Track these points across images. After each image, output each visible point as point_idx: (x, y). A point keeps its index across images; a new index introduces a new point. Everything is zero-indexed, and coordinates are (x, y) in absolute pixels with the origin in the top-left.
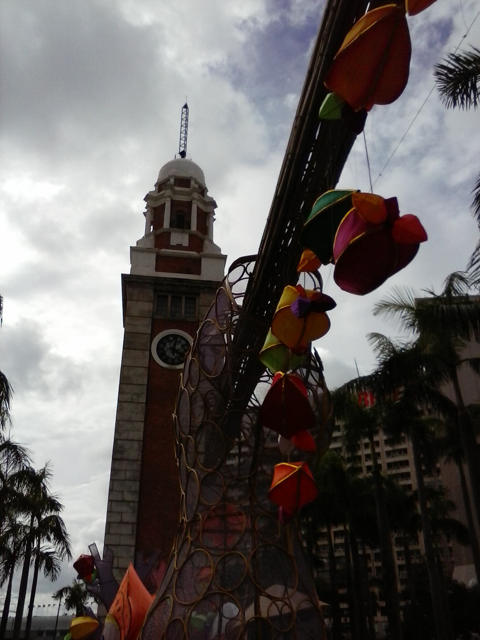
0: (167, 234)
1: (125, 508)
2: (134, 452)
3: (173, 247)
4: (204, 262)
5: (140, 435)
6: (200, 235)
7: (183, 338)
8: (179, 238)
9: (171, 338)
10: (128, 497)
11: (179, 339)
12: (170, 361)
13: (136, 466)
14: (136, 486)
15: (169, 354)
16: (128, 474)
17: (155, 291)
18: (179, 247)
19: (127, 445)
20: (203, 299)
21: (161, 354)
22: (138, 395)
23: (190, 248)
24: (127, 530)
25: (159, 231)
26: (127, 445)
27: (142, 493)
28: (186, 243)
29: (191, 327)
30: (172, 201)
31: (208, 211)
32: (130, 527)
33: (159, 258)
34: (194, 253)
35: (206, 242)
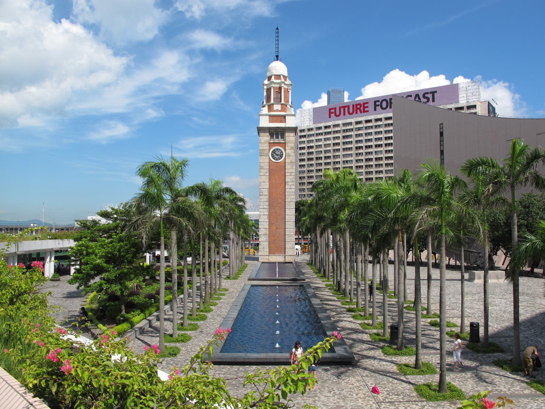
1: (264, 210)
3: (275, 111)
5: (268, 187)
6: (286, 103)
8: (277, 107)
10: (265, 207)
13: (267, 197)
15: (275, 156)
16: (265, 200)
18: (277, 111)
20: (287, 134)
21: (273, 157)
22: (266, 173)
23: (282, 110)
24: (266, 217)
25: (269, 104)
27: (270, 205)
28: (280, 109)
34: (283, 113)
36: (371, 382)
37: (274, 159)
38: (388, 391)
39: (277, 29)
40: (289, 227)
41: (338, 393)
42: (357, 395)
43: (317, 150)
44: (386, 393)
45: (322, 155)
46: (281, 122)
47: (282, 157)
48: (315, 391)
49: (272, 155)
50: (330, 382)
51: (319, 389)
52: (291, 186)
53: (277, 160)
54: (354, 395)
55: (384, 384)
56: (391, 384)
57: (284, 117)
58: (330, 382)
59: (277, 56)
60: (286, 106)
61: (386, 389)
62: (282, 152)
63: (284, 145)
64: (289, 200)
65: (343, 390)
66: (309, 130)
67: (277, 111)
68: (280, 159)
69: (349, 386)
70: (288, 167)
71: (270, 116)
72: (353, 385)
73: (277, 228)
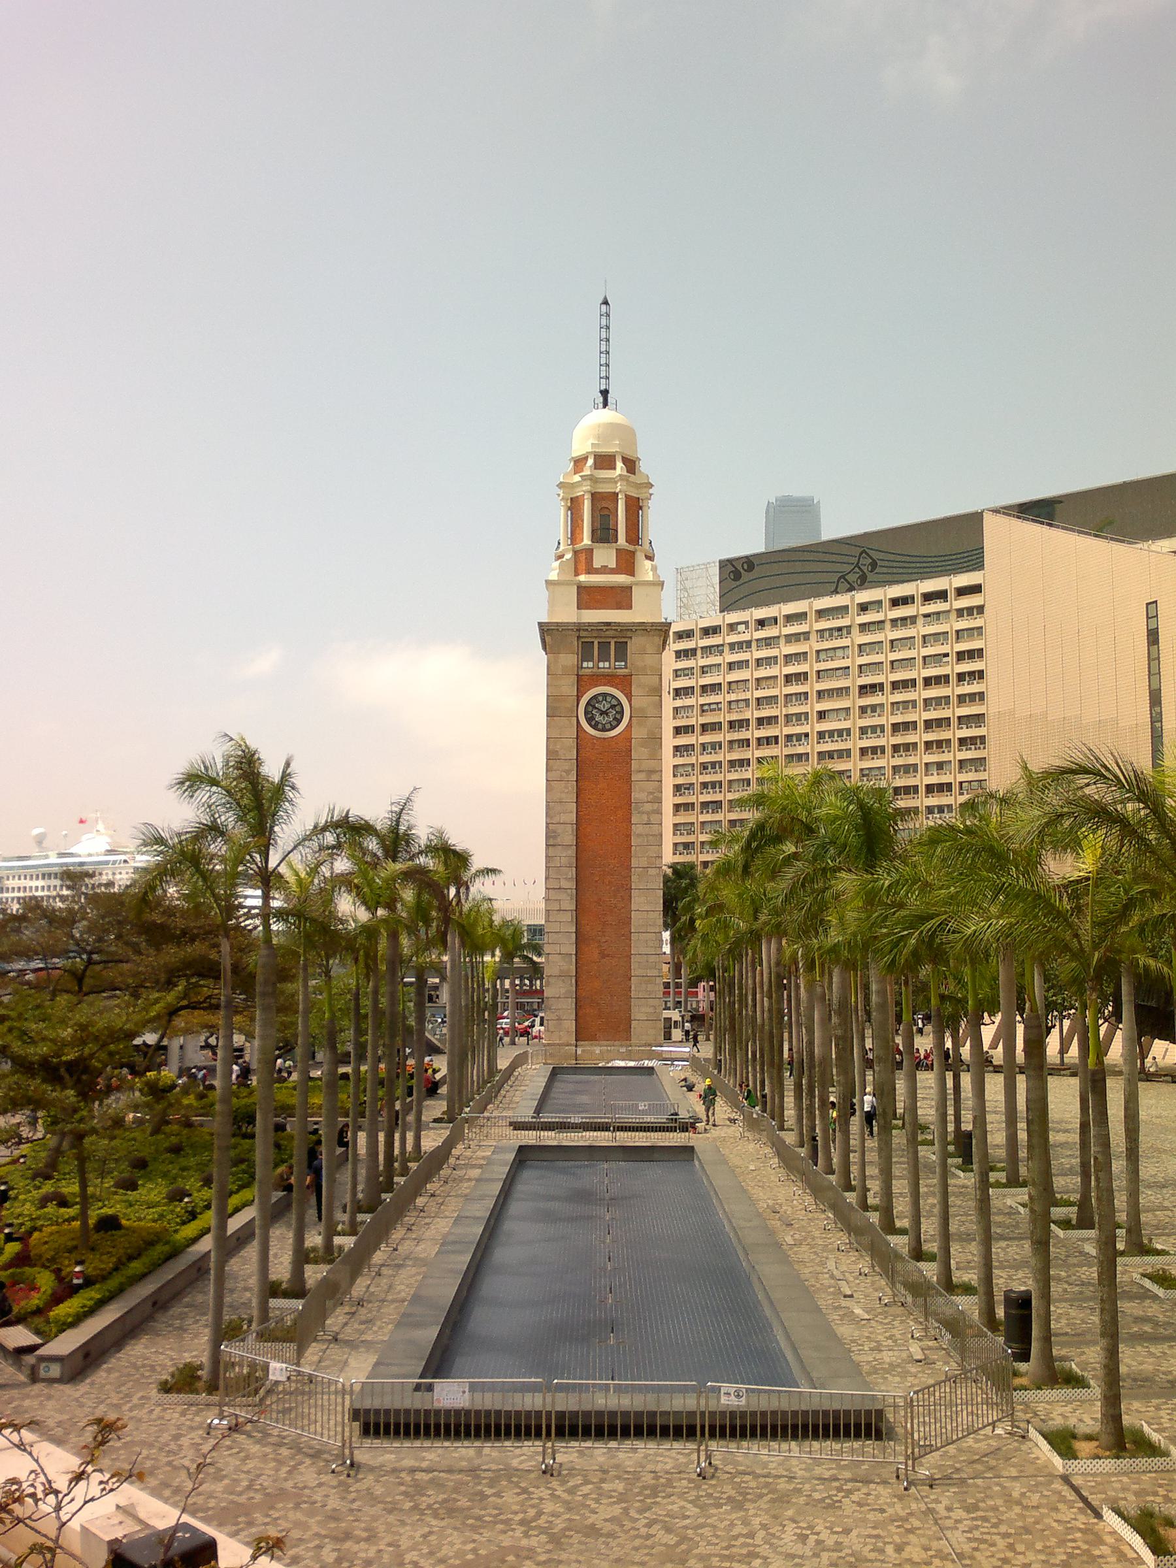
0: (589, 552)
1: (563, 896)
2: (568, 837)
4: (635, 591)
5: (573, 817)
6: (631, 548)
7: (613, 697)
8: (605, 556)
9: (600, 698)
10: (565, 884)
11: (609, 699)
12: (600, 726)
13: (572, 852)
14: (572, 872)
17: (579, 637)
18: (604, 570)
19: (560, 829)
21: (590, 720)
22: (568, 772)
24: (568, 917)
26: (560, 829)
29: (624, 683)
30: (594, 496)
31: (640, 496)
32: (569, 914)
33: (582, 589)
34: (621, 579)
35: (640, 556)
36: (945, 1502)
37: (595, 727)
38: (1006, 1535)
39: (606, 302)
40: (643, 950)
41: (830, 1541)
42: (899, 1549)
43: (733, 697)
44: (1001, 1543)
45: (747, 715)
46: (619, 606)
47: (619, 721)
48: (751, 1535)
49: (586, 713)
50: (802, 1500)
51: (764, 1526)
52: (648, 813)
53: (604, 730)
54: (890, 1549)
55: (995, 1509)
56: (1017, 1509)
57: (627, 590)
58: (802, 1500)
59: (605, 393)
60: (633, 553)
61: (1003, 1529)
62: (620, 704)
63: (624, 683)
64: (644, 862)
65: (847, 1531)
66: (707, 632)
67: (604, 570)
68: (613, 728)
69: (871, 1516)
70: (639, 753)
71: (582, 589)
72: (882, 1511)
73: (603, 955)
